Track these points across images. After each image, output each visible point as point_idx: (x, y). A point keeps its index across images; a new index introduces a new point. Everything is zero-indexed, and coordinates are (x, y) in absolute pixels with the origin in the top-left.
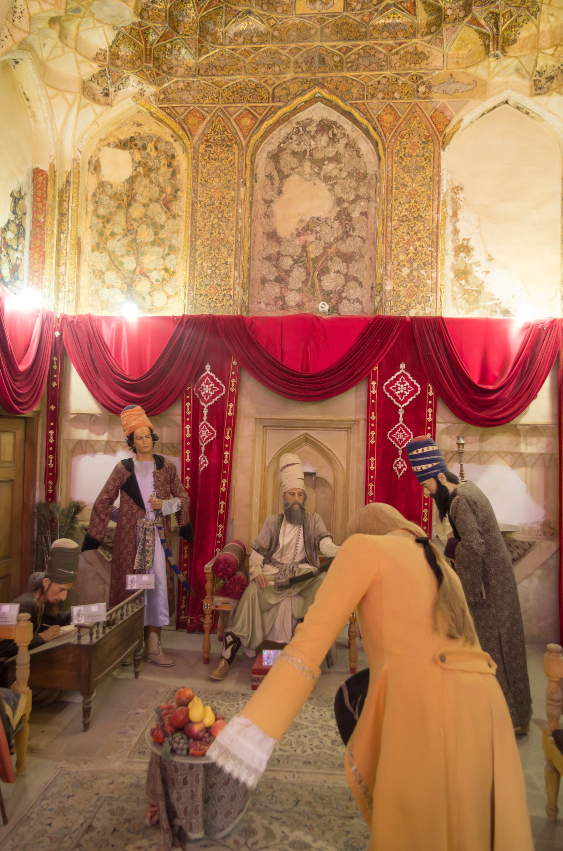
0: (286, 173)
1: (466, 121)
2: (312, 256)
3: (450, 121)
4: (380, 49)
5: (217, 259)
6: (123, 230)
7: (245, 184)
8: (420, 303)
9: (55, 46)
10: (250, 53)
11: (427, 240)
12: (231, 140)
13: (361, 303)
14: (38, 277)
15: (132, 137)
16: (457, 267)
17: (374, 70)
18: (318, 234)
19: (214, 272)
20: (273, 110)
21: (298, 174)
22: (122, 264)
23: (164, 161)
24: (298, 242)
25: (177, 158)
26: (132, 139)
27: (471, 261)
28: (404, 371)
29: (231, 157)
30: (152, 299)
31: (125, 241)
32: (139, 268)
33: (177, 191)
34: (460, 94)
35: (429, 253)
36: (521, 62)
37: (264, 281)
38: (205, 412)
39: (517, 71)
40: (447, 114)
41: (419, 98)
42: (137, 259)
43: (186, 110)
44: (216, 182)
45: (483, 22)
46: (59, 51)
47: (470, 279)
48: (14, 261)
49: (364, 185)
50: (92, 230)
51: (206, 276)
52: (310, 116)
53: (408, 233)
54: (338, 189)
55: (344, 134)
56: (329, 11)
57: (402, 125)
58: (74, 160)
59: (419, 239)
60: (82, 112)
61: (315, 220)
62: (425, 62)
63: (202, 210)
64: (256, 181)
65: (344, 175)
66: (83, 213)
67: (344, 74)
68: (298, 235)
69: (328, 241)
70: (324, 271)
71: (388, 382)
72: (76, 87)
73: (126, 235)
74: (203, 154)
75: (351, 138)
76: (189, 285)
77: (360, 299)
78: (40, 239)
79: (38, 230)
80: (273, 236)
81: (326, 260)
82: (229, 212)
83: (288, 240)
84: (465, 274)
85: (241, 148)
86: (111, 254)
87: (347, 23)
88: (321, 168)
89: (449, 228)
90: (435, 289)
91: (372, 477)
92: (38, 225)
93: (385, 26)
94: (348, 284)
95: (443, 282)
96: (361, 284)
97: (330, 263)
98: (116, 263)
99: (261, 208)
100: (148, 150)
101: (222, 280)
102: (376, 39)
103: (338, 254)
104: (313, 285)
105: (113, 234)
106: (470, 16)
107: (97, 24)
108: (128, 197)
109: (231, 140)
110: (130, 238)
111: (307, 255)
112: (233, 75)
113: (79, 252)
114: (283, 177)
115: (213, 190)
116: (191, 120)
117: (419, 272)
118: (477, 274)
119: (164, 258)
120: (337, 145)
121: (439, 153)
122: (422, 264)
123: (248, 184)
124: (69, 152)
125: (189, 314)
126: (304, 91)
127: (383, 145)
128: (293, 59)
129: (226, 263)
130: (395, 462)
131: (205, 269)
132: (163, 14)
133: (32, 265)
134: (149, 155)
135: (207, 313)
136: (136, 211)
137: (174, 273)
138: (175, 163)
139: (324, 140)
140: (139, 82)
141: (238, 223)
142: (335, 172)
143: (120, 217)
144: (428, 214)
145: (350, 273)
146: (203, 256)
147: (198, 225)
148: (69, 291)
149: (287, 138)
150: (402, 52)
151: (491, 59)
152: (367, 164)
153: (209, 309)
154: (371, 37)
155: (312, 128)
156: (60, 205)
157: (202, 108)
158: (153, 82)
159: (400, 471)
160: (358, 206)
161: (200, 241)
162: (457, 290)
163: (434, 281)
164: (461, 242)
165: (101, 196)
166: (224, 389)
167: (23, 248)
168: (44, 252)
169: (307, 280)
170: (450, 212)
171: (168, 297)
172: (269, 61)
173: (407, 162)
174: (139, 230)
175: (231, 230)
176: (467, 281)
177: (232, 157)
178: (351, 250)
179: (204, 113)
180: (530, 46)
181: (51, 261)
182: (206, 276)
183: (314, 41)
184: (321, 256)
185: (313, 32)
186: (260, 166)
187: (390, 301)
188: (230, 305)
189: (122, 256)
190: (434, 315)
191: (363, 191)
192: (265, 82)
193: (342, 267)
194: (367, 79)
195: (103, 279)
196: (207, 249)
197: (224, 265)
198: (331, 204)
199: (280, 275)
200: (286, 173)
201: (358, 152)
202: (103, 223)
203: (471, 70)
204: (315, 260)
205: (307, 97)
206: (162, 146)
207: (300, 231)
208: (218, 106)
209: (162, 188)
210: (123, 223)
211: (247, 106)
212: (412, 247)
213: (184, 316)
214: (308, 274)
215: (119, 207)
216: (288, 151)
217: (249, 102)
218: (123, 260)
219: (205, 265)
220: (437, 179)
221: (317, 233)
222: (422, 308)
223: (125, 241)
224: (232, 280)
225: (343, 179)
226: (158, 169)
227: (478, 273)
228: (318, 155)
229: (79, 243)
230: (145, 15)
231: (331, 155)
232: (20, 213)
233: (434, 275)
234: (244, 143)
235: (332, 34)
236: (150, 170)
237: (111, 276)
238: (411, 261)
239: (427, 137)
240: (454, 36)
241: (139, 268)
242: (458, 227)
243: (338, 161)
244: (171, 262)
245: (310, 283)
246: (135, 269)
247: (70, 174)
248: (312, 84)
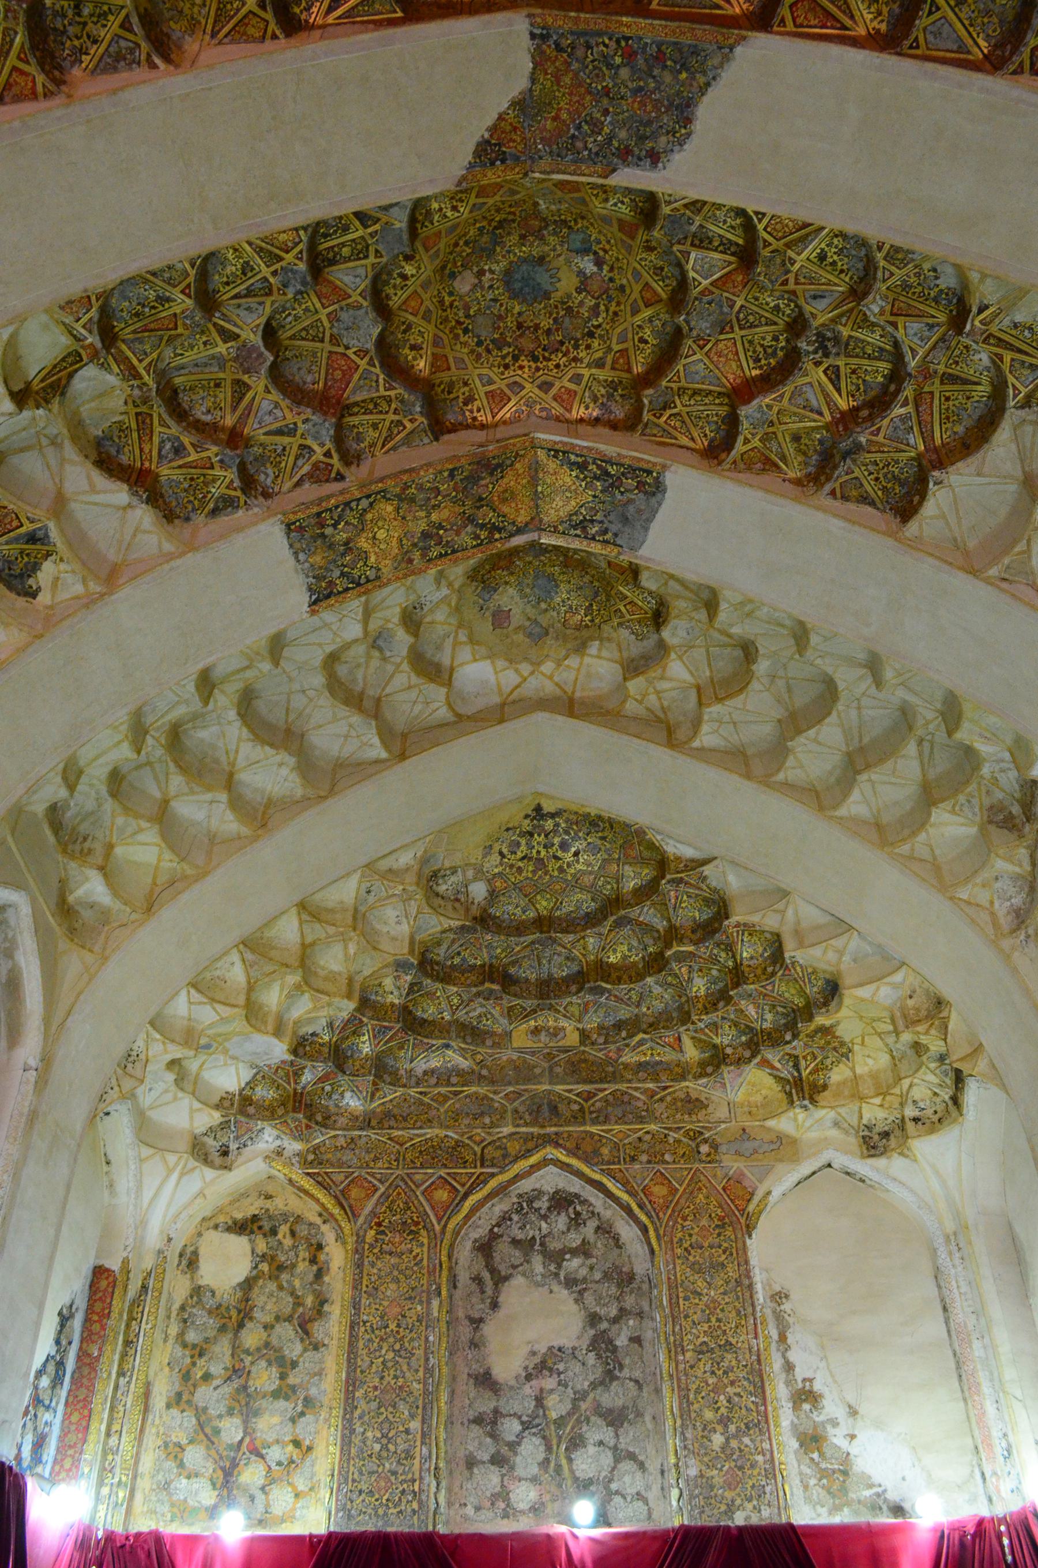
0: (503, 1273)
1: (776, 1193)
2: (554, 1415)
3: (752, 1194)
4: (637, 1094)
5: (391, 1423)
6: (226, 1369)
7: (439, 1294)
8: (750, 1500)
9: (166, 1091)
10: (446, 1098)
11: (745, 1383)
12: (417, 1224)
13: (646, 1502)
14: (73, 1457)
15: (255, 1216)
16: (801, 1429)
17: (631, 1123)
18: (562, 1376)
19: (385, 1448)
20: (482, 1178)
21: (524, 1275)
22: (217, 1431)
23: (304, 1254)
24: (527, 1390)
25: (326, 1249)
26: (255, 1218)
27: (821, 1418)
29: (416, 1250)
30: (267, 1500)
31: (227, 1389)
32: (247, 1440)
33: (323, 1302)
34: (761, 1157)
35: (753, 1407)
36: (839, 1114)
37: (471, 1463)
39: (836, 1124)
40: (746, 1183)
41: (701, 1161)
42: (246, 1422)
43: (347, 1177)
44: (391, 1290)
45: (778, 1065)
46: (169, 1096)
48: (39, 1430)
49: (631, 1292)
50: (172, 1369)
51: (370, 1456)
52: (538, 1186)
53: (713, 1373)
54: (589, 1298)
55: (593, 1213)
56: (560, 1044)
57: (682, 1201)
58: (160, 1252)
59: (732, 1383)
60: (185, 1179)
61: (555, 1351)
62: (704, 1112)
63: (367, 1337)
64: (455, 1287)
65: (598, 1276)
66: (159, 1336)
67: (588, 1128)
68: (529, 1377)
69: (579, 1387)
70: (576, 1443)
72: (184, 1145)
73: (229, 1378)
74: (372, 1246)
75: (604, 1219)
76: (340, 1472)
77: (643, 1493)
78: (87, 1388)
79: (86, 1371)
80: (485, 1380)
81: (579, 1421)
82: (412, 1340)
83: (512, 1388)
84: (817, 1441)
85: (433, 1237)
86: (200, 1413)
87: (585, 1061)
88: (559, 1266)
89: (777, 1364)
90: (771, 1472)
92: (87, 1363)
93: (641, 1066)
94: (620, 1466)
95: (783, 1459)
96: (642, 1466)
97: (585, 1428)
98: (208, 1430)
99: (465, 1331)
100: (280, 1236)
101: (399, 1462)
102: (630, 1081)
103: (599, 1410)
104: (558, 1468)
105: (207, 1377)
106: (759, 1057)
107: (229, 1062)
108: (239, 1311)
109: (417, 1224)
110: (236, 1383)
111: (544, 1414)
112: (421, 1128)
113: (146, 1410)
114: (500, 1280)
115: (386, 1303)
116: (355, 1193)
117: (741, 1442)
118: (835, 1441)
119: (293, 1420)
120: (582, 1229)
121: (744, 1243)
122: (743, 1427)
123: (444, 1292)
124: (153, 1239)
125: (338, 1530)
126: (529, 1151)
127: (656, 1230)
128: (509, 1108)
129: (407, 1432)
131: (369, 1443)
132: (326, 1050)
133: (64, 1433)
134: (280, 1243)
135: (370, 1528)
136: (252, 1337)
137: (310, 1449)
138: (322, 1257)
139: (561, 1222)
140: (278, 1137)
141: (427, 1360)
142: (583, 1272)
143: (223, 1348)
144: (741, 1340)
145: (622, 1446)
146: (366, 1418)
147: (359, 1363)
148: (120, 1482)
149: (504, 1218)
150: (669, 1098)
151: (798, 1110)
152: (633, 1259)
153: (374, 1519)
154: (622, 1079)
155: (543, 1204)
156: (128, 1326)
157: (373, 1175)
158: (299, 1138)
160: (625, 1328)
161: (362, 1391)
162: (809, 1471)
163: (768, 1456)
164: (800, 1385)
165: (194, 1310)
167: (57, 1403)
168: (90, 1411)
169: (547, 1460)
170: (774, 1334)
171: (297, 1496)
172: (475, 1109)
173: (695, 1256)
174: (254, 1369)
175: (417, 1371)
177: (419, 1250)
178: (619, 1403)
179: (376, 1182)
180: (846, 1093)
181: (98, 1427)
182: (370, 1456)
183: (540, 1083)
184: (569, 1414)
185: (537, 1071)
186: (461, 1262)
187: (697, 1496)
188: (414, 1511)
189: (220, 1416)
191: (629, 1301)
192: (469, 1138)
193: (607, 1434)
194: (621, 1136)
195: (182, 1460)
196: (374, 1405)
197: (404, 1435)
198: (581, 1325)
199: (498, 1452)
200: (503, 1273)
201: (616, 1239)
202: (192, 1357)
203: (771, 1123)
204: (560, 1422)
205: (533, 1160)
206: (302, 1230)
207: (530, 1370)
208: (398, 1172)
209: (298, 1297)
210: (227, 1360)
211: (442, 1172)
212: (722, 1397)
213: (330, 1535)
214: (549, 1448)
215: (223, 1329)
216: (505, 1238)
217: (445, 1166)
218: (221, 1425)
219: (369, 1434)
220: (746, 1282)
221: (559, 1374)
222: (754, 1507)
223: (227, 1389)
224: (417, 1462)
225: (597, 1282)
226: (294, 1266)
227: (837, 1438)
228: (554, 1245)
229: (147, 1395)
230: (301, 1051)
231: (574, 1245)
232: (64, 1342)
233: (766, 1446)
234: (437, 1228)
235: (566, 1074)
236: (281, 1268)
237: (195, 1456)
238: (725, 1421)
239: (721, 1219)
240: (741, 1080)
241: (247, 1440)
242: (791, 1359)
243: (587, 1255)
244: (305, 1428)
245: (552, 1465)
246: (241, 1442)
247: (149, 1274)
248: (540, 1141)
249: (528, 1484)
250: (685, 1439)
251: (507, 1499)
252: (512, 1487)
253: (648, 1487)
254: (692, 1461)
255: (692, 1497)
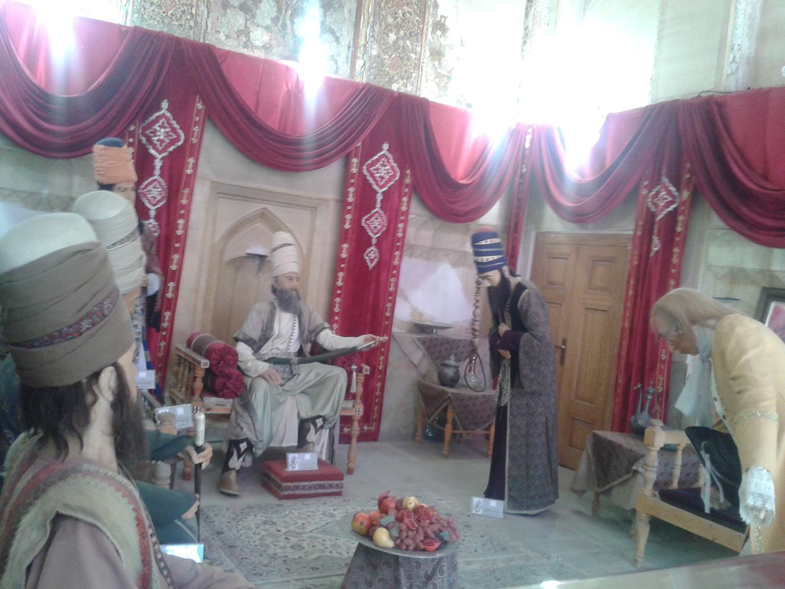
11: (415, 7)
28: (387, 152)
35: (416, 23)
38: (158, 164)
47: (444, 61)
71: (370, 162)
77: (335, 57)
84: (439, 55)
90: (418, 67)
91: (343, 266)
104: (284, 25)
130: (367, 252)
153: (161, 25)
159: (372, 261)
164: (439, 19)
166: (183, 138)
176: (440, 63)
187: (374, 68)
188: (191, 27)
190: (413, 93)
212: (400, 12)
214: (279, 10)
222: (404, 83)
233: (418, 49)
238: (398, 27)
245: (281, 22)
249: (262, 30)
250: (374, 31)
251: (248, 36)
252: (252, 29)
253: (339, 54)
254: (375, 46)
255: (371, 68)
